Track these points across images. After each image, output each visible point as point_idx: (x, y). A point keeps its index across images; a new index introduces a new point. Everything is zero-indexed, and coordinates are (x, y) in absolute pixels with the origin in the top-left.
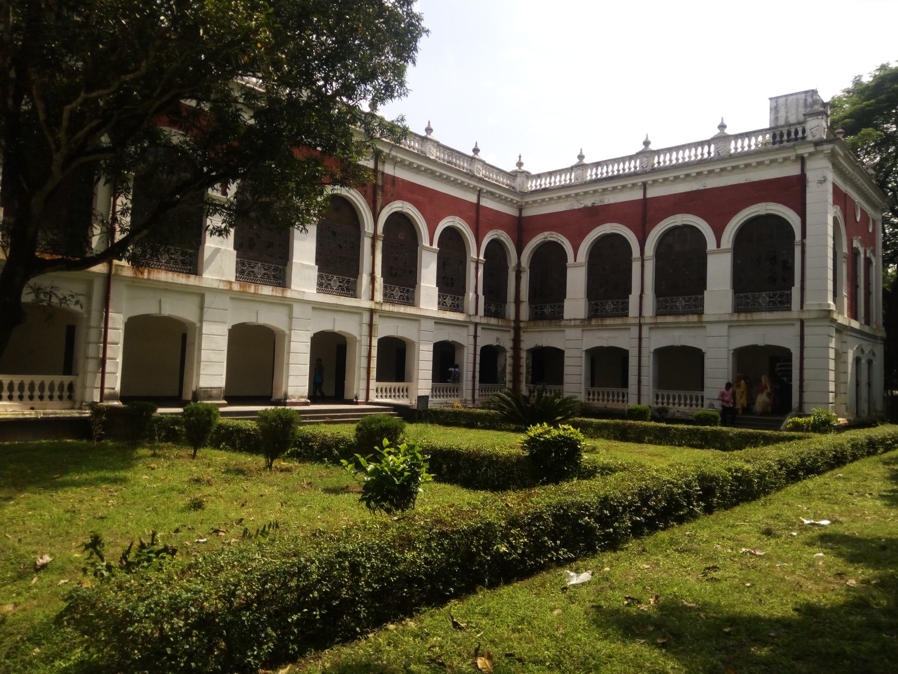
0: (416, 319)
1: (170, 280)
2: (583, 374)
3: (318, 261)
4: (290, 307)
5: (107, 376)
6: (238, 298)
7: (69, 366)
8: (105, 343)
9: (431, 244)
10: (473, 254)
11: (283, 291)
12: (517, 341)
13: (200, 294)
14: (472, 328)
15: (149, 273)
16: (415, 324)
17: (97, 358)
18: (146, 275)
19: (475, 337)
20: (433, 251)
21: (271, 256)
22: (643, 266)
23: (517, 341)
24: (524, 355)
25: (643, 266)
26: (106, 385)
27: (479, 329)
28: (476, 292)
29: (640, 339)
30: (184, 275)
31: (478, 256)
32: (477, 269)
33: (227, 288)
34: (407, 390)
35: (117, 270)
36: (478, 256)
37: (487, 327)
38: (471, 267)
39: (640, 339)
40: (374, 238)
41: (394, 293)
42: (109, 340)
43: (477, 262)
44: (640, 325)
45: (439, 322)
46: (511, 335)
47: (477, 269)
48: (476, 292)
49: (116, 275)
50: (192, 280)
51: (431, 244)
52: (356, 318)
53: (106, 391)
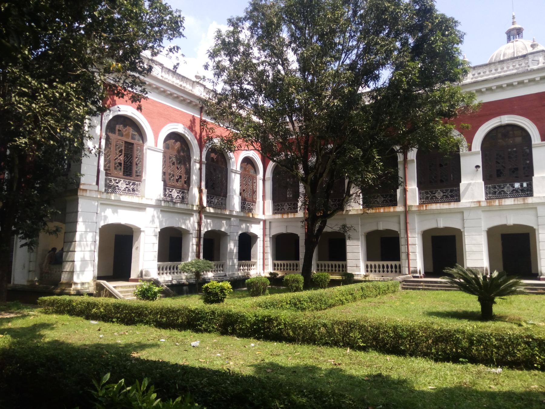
1: (439, 208)
3: (484, 180)
4: (536, 208)
5: (410, 261)
6: (488, 210)
7: (397, 258)
8: (408, 245)
11: (524, 200)
13: (461, 212)
15: (426, 206)
17: (406, 252)
18: (424, 207)
21: (517, 177)
26: (411, 266)
30: (447, 204)
33: (477, 205)
35: (409, 208)
42: (410, 243)
49: (409, 210)
50: (453, 205)
53: (411, 269)
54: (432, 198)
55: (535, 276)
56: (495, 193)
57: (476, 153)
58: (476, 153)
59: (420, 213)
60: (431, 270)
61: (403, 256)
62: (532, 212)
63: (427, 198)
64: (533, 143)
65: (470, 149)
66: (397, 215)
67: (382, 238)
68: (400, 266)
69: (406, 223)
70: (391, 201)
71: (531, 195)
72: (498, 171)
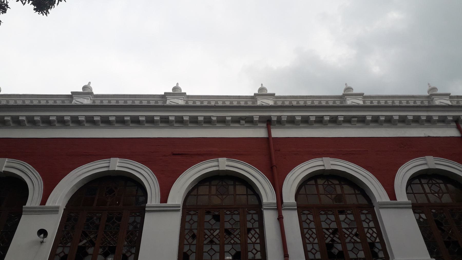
9: (392, 196)
40: (279, 205)
51: (392, 196)
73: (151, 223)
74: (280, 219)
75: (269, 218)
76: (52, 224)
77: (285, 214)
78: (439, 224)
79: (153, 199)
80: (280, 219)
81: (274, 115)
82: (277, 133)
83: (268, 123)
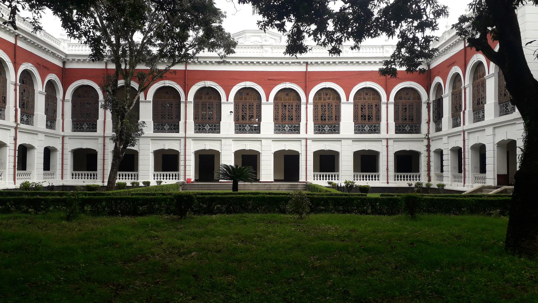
0: (339, 140)
2: (450, 164)
9: (348, 100)
10: (384, 98)
12: (428, 146)
14: (384, 142)
16: (340, 142)
19: (387, 146)
20: (350, 103)
22: (465, 93)
23: (428, 146)
24: (432, 154)
25: (465, 93)
27: (391, 142)
28: (387, 121)
29: (464, 141)
31: (388, 99)
32: (387, 107)
34: (338, 176)
36: (388, 99)
37: (396, 140)
38: (383, 108)
39: (464, 141)
41: (325, 128)
43: (387, 104)
44: (464, 132)
45: (355, 140)
46: (426, 142)
47: (387, 107)
48: (387, 121)
52: (299, 142)
54: (203, 130)
55: (258, 180)
56: (240, 129)
57: (231, 103)
58: (231, 103)
59: (195, 139)
60: (198, 178)
61: (182, 168)
62: (259, 142)
63: (200, 129)
64: (262, 102)
65: (227, 100)
66: (178, 139)
67: (163, 155)
68: (179, 175)
69: (185, 145)
70: (174, 129)
71: (259, 132)
72: (243, 116)
73: (263, 107)
74: (307, 108)
75: (303, 107)
76: (231, 108)
77: (308, 105)
78: (362, 109)
79: (264, 100)
80: (307, 108)
81: (309, 61)
82: (311, 69)
83: (307, 63)
